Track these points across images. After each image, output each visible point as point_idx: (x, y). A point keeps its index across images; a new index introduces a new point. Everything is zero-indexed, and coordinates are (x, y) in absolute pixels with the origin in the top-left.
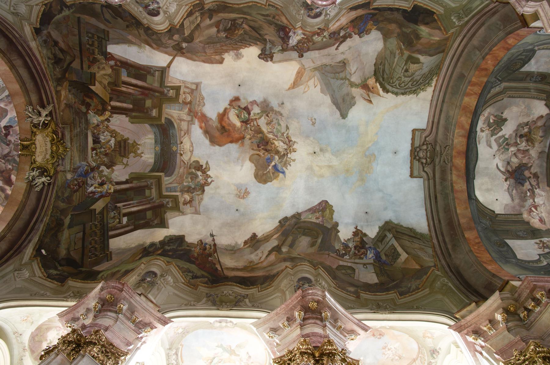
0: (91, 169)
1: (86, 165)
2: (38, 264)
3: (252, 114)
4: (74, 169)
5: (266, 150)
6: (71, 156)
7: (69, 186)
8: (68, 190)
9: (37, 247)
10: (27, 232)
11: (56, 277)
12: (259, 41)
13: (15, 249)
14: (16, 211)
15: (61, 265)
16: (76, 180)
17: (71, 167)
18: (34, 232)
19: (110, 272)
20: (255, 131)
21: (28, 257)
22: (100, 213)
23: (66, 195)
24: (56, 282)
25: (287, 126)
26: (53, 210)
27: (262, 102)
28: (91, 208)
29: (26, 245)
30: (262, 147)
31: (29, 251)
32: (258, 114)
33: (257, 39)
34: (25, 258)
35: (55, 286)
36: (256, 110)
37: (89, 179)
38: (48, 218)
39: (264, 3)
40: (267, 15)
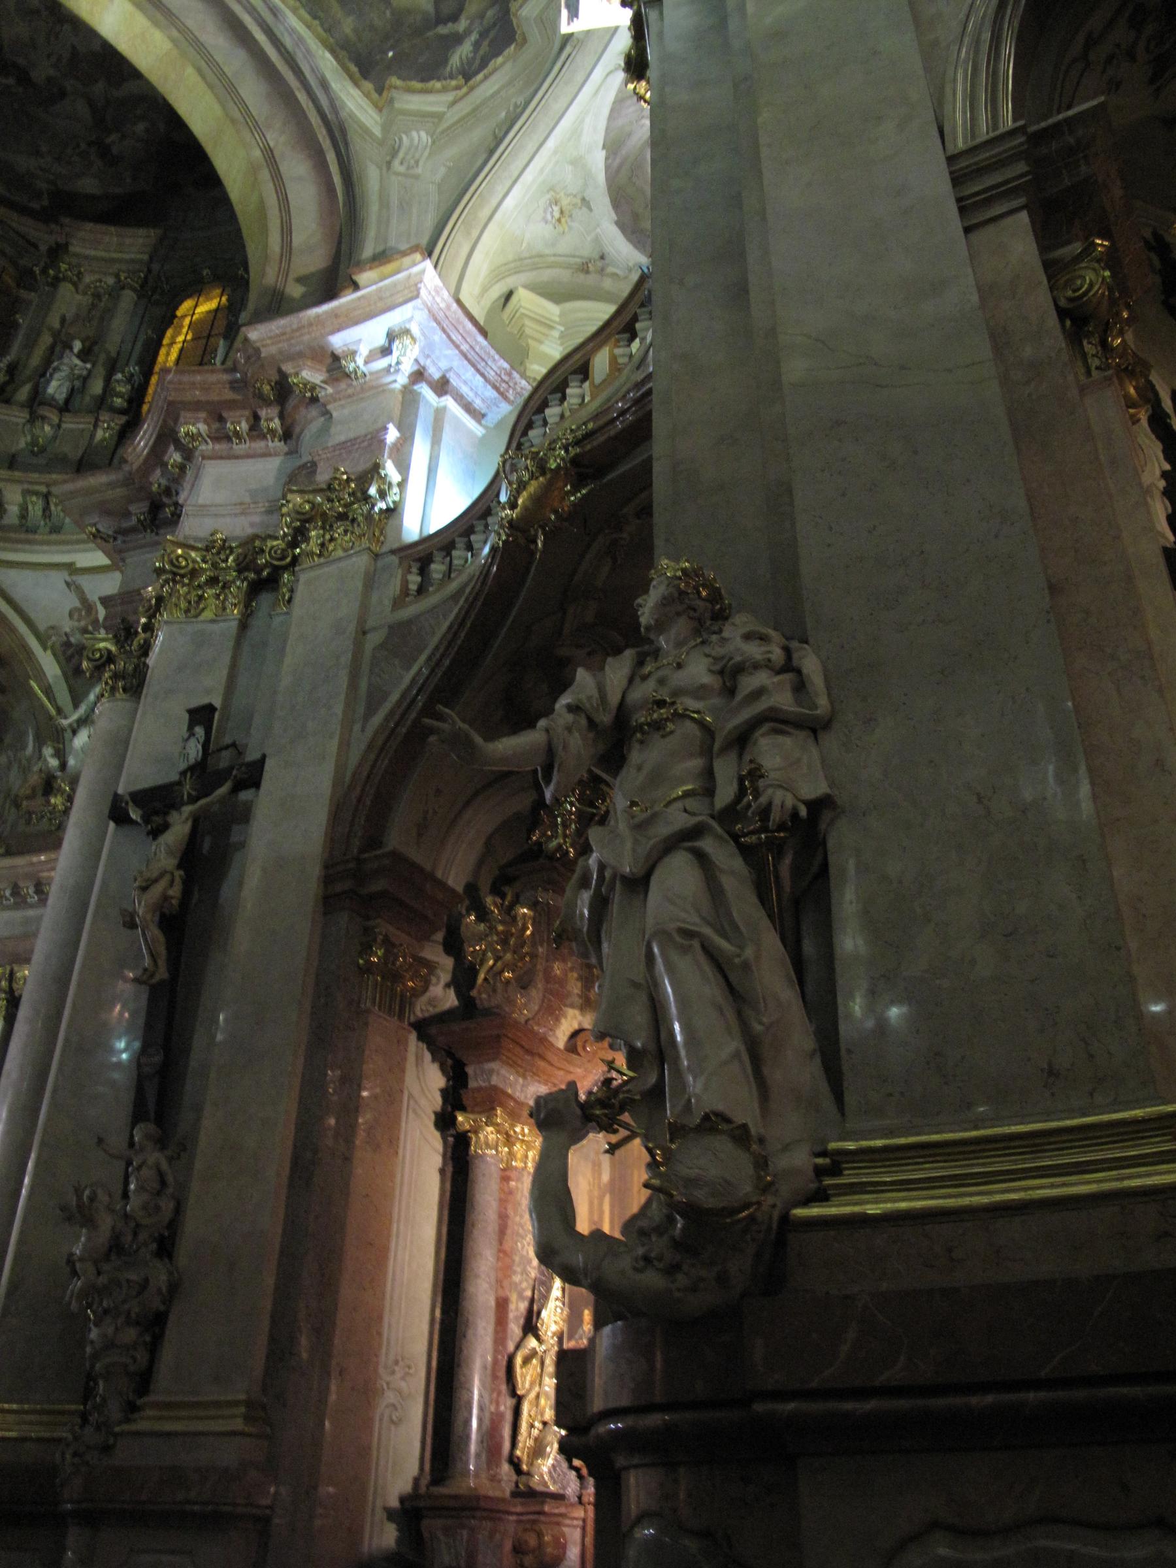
2: (410, 91)
9: (354, 68)
11: (481, 52)
13: (326, 144)
14: (203, 77)
15: (454, 18)
21: (372, 111)
24: (500, 60)
29: (332, 102)
31: (354, 101)
35: (509, 65)
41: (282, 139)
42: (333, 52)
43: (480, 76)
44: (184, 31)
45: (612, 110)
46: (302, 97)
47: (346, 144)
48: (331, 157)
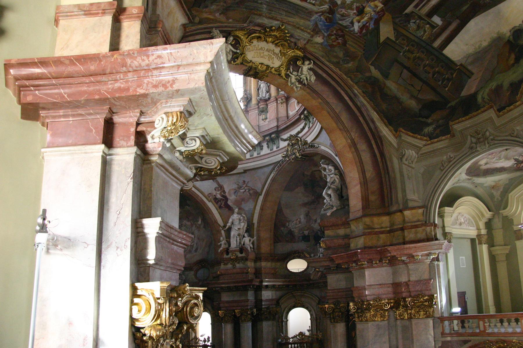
0: (329, 13)
1: (320, 16)
4: (314, 30)
6: (294, 26)
7: (332, 46)
8: (336, 49)
10: (358, 114)
14: (330, 115)
15: (427, 117)
16: (330, 35)
17: (309, 33)
18: (363, 109)
19: (487, 90)
22: (397, 38)
23: (341, 55)
24: (444, 138)
26: (350, 77)
28: (381, 40)
29: (376, 127)
31: (385, 131)
34: (393, 142)
35: (447, 141)
37: (340, 22)
38: (356, 87)
41: (356, 135)
42: (377, 113)
43: (436, 140)
44: (323, 99)
45: (508, 202)
46: (361, 119)
47: (381, 142)
48: (373, 142)
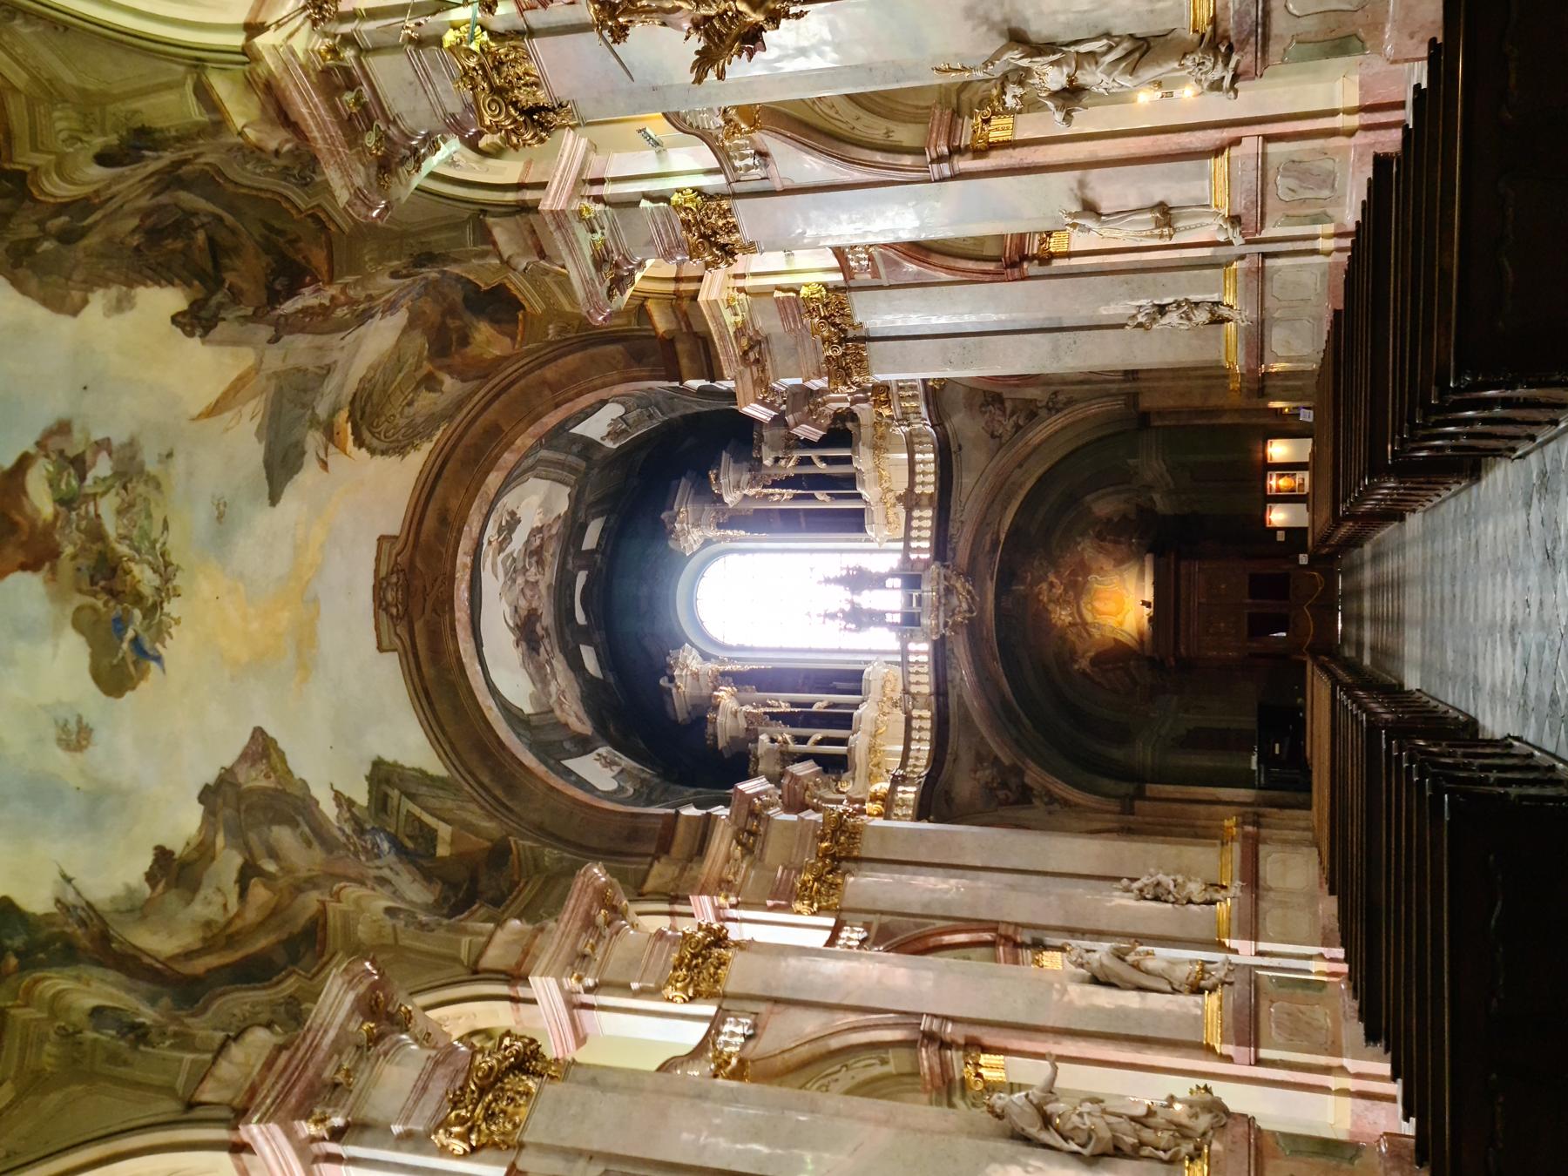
3: (89, 481)
5: (113, 594)
12: (202, 282)
20: (85, 532)
25: (165, 521)
27: (123, 447)
30: (102, 583)
32: (104, 479)
33: (201, 275)
36: (102, 467)
39: (303, 206)
40: (281, 233)
